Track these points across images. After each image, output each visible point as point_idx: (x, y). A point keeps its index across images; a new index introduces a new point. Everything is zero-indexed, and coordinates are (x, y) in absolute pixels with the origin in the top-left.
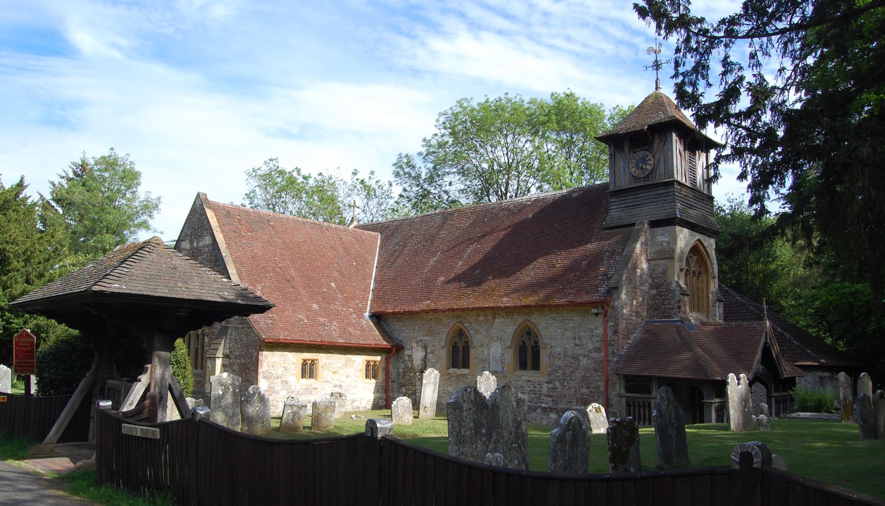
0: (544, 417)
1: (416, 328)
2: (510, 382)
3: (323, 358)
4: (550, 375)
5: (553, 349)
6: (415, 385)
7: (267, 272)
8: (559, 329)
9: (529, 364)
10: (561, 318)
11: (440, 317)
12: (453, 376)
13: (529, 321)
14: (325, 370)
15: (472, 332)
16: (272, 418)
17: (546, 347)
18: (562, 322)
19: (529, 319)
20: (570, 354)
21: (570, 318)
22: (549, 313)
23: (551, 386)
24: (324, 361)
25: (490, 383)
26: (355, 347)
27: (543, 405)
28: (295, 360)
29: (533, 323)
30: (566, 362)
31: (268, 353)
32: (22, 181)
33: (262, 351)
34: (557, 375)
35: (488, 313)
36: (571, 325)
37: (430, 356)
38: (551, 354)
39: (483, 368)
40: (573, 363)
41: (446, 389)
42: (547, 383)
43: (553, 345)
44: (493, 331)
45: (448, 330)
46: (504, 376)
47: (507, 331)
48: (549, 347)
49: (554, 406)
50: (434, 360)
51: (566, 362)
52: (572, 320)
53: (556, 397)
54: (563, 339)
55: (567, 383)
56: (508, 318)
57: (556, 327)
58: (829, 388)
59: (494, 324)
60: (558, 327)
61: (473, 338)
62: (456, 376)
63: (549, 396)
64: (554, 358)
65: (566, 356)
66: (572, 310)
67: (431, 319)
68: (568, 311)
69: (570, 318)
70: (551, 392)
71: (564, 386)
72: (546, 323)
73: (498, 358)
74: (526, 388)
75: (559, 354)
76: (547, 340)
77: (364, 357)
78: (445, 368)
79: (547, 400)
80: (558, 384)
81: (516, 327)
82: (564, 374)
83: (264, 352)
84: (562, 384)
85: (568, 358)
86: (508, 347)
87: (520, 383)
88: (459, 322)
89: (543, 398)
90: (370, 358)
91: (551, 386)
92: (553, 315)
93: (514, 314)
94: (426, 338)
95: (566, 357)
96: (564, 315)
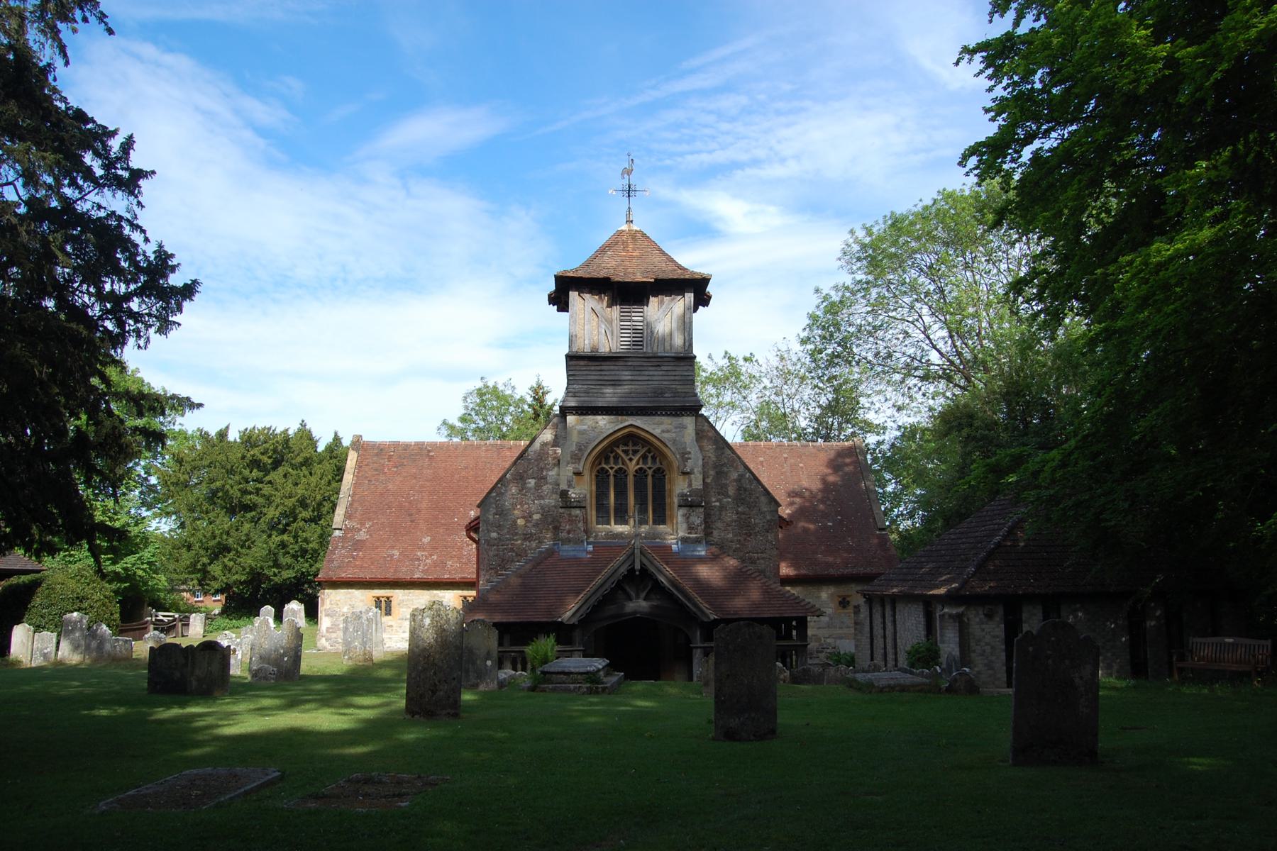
3: (398, 595)
7: (390, 508)
14: (402, 607)
16: (872, 659)
24: (400, 598)
25: (361, 622)
26: (442, 582)
28: (363, 598)
31: (331, 591)
32: (336, 434)
33: (324, 589)
58: (952, 635)
77: (455, 591)
83: (326, 591)
90: (465, 593)
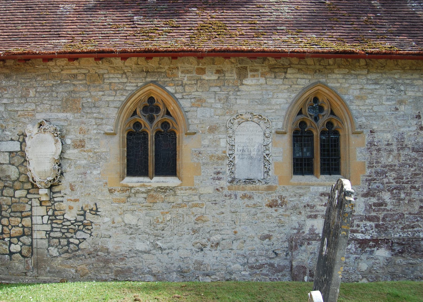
0: (364, 257)
1: (32, 93)
2: (281, 197)
4: (370, 181)
5: (375, 135)
6: (31, 216)
8: (388, 100)
9: (317, 164)
10: (389, 82)
11: (102, 72)
12: (137, 192)
13: (325, 86)
15: (186, 104)
17: (361, 133)
18: (393, 88)
19: (323, 80)
20: (409, 143)
21: (408, 81)
22: (365, 72)
23: (374, 200)
27: (359, 236)
29: (331, 89)
30: (402, 158)
34: (386, 180)
35: (227, 65)
36: (410, 93)
37: (71, 153)
38: (371, 144)
39: (218, 173)
40: (416, 159)
41: (118, 219)
42: (365, 195)
43: (375, 127)
44: (238, 101)
45: (123, 99)
46: (270, 188)
47: (273, 101)
48: (366, 132)
49: (383, 236)
50: (84, 162)
51: (402, 158)
52: (412, 85)
53: (384, 219)
54: (396, 118)
55: (407, 194)
56: (275, 77)
57: (381, 96)
59: (242, 88)
60: (384, 97)
61: (189, 115)
62: (148, 192)
63: (370, 219)
64: (379, 150)
65: (402, 147)
66: (410, 69)
67: (75, 76)
68: (403, 69)
69: (408, 81)
70: (374, 210)
71: (400, 200)
72: (361, 89)
73: (254, 153)
74: (319, 208)
75: (388, 145)
76: (364, 120)
78: (117, 176)
79: (365, 226)
80: (386, 196)
81: (293, 95)
82: (399, 178)
84: (393, 196)
85: (406, 152)
86: (277, 133)
87: (306, 199)
88: (154, 82)
89: (356, 222)
91: (374, 200)
92: (373, 76)
93: (289, 71)
94: (61, 115)
95: (403, 148)
96: (396, 77)
